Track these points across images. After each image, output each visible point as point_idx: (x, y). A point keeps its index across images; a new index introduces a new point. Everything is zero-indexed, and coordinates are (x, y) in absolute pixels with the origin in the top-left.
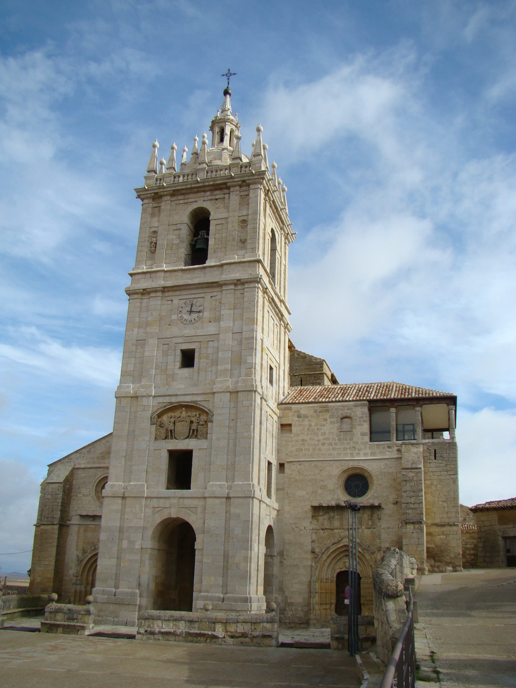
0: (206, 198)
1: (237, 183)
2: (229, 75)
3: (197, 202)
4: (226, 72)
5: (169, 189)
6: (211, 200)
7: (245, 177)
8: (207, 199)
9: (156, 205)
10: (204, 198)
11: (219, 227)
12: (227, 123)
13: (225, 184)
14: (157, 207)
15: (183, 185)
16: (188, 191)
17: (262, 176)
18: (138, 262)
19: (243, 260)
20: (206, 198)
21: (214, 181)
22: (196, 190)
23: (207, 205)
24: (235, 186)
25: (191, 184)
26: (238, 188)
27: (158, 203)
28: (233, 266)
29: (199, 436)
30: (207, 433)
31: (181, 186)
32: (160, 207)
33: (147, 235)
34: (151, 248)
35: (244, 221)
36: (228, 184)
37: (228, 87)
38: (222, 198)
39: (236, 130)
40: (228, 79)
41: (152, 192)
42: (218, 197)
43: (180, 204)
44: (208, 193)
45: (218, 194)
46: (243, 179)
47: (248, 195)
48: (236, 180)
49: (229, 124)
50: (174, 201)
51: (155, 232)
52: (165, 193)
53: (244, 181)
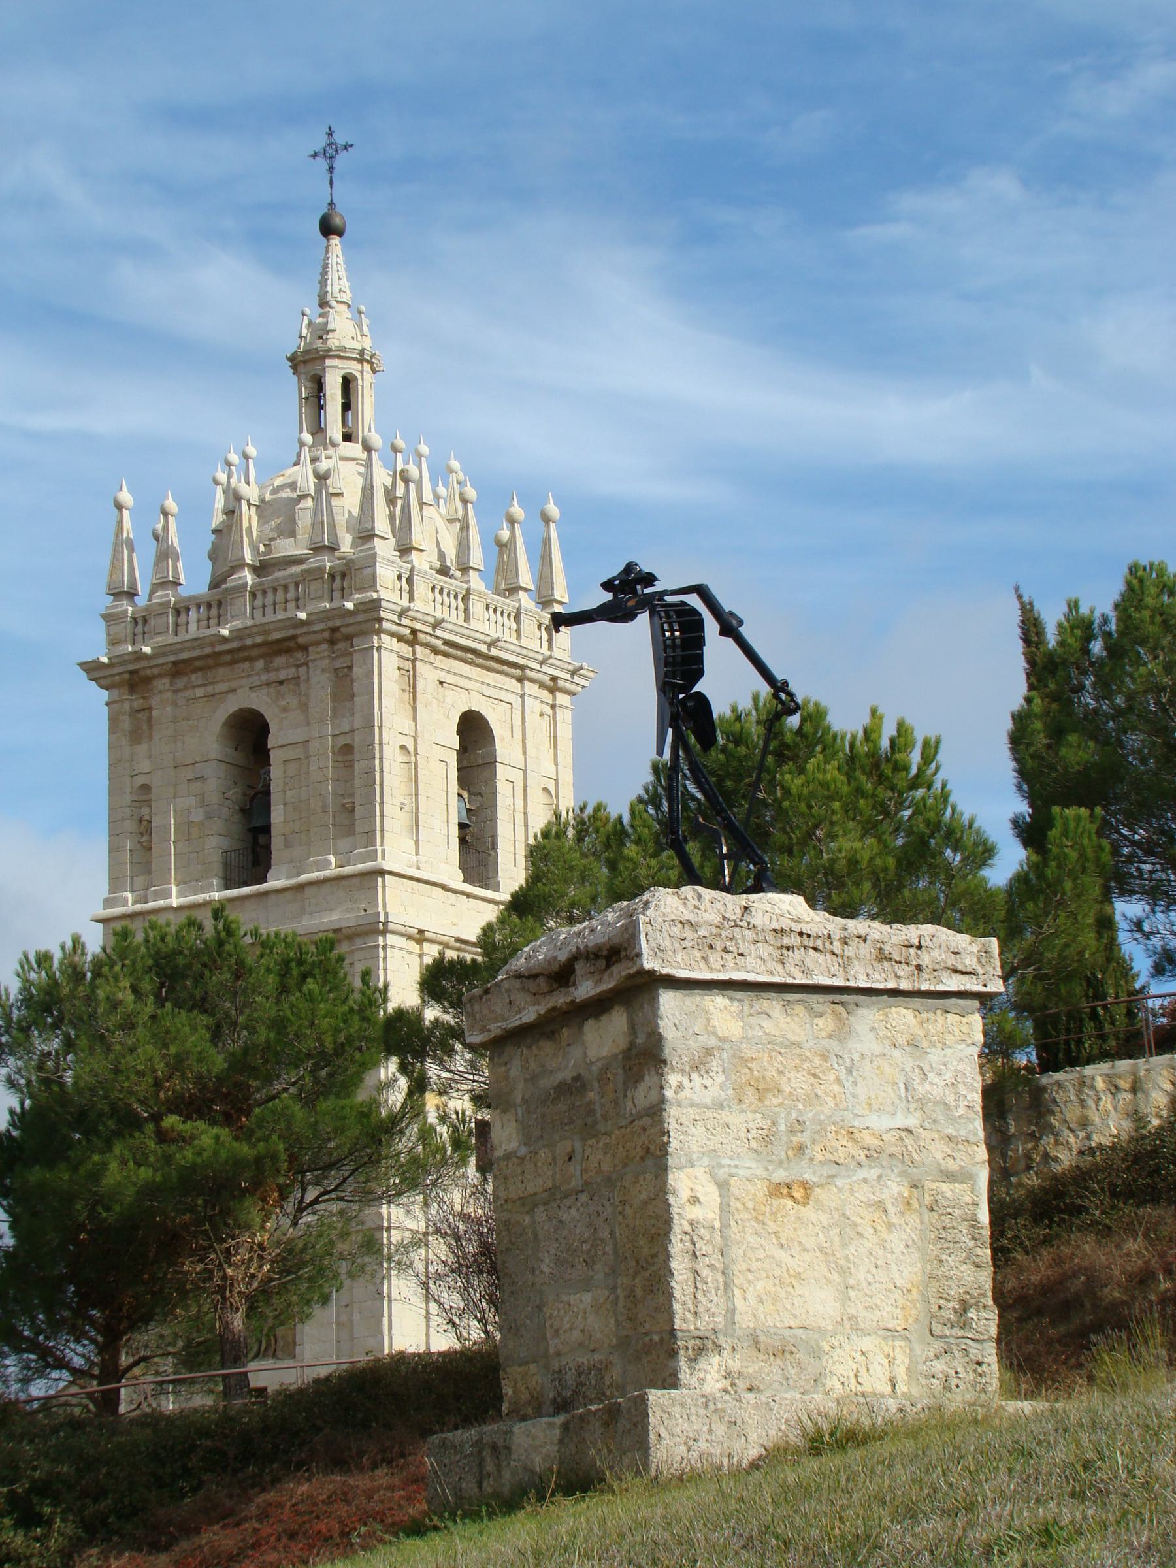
0: (255, 680)
1: (319, 637)
2: (331, 151)
3: (234, 690)
4: (320, 142)
5: (161, 661)
6: (268, 684)
7: (334, 618)
8: (259, 683)
9: (138, 704)
10: (252, 680)
11: (292, 769)
12: (328, 362)
13: (293, 638)
14: (143, 710)
15: (194, 648)
16: (211, 662)
17: (374, 615)
18: (116, 883)
19: (347, 870)
20: (255, 680)
21: (265, 633)
22: (228, 658)
23: (260, 701)
24: (318, 643)
25: (212, 645)
26: (325, 646)
27: (143, 698)
28: (326, 888)
29: (279, 1353)
30: (295, 1344)
31: (189, 650)
32: (150, 709)
33: (128, 798)
34: (142, 834)
35: (348, 749)
36: (301, 640)
37: (331, 204)
38: (293, 678)
39: (362, 372)
40: (331, 169)
41: (121, 669)
42: (282, 675)
43: (195, 699)
44: (260, 664)
45: (283, 667)
46: (330, 624)
47: (350, 668)
48: (316, 628)
49: (336, 362)
50: (180, 690)
51: (146, 788)
52: (156, 671)
53: (334, 630)
